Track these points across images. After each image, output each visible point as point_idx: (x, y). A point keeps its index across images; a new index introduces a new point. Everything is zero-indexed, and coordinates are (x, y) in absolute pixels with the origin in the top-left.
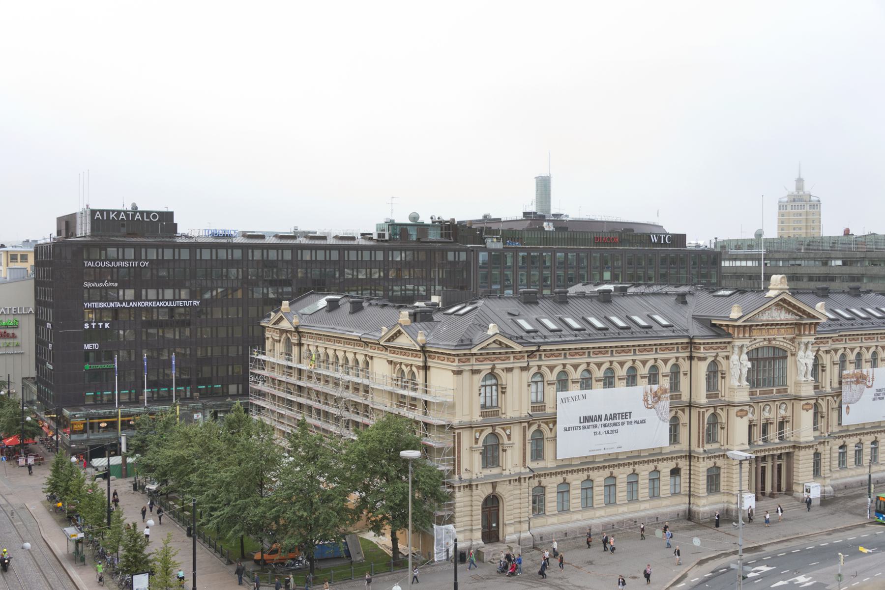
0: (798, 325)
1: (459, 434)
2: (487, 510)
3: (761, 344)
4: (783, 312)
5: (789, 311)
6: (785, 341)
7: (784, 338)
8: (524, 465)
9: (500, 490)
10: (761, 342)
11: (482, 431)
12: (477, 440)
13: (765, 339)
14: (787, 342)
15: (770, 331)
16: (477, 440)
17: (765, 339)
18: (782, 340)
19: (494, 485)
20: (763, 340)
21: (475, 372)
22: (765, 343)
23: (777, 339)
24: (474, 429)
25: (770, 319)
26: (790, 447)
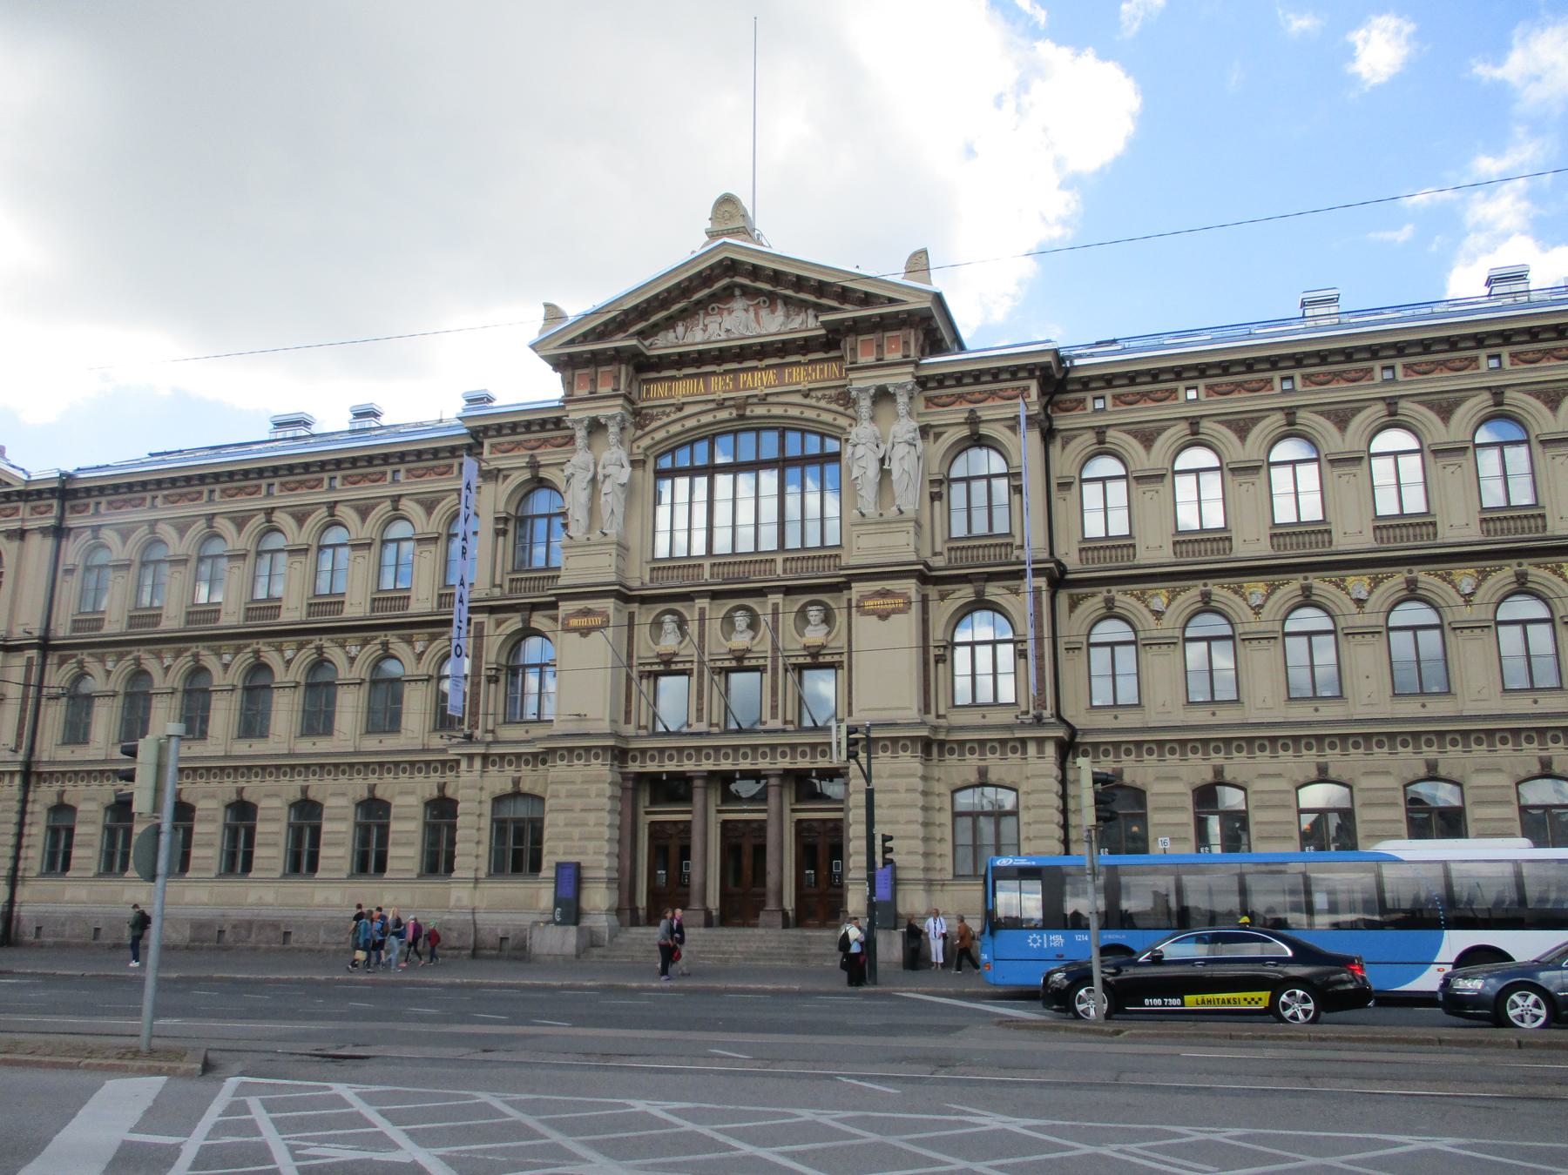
4: (780, 311)
6: (807, 401)
7: (806, 394)
13: (721, 405)
14: (823, 404)
17: (721, 405)
18: (797, 399)
22: (723, 415)
23: (770, 399)
25: (724, 336)
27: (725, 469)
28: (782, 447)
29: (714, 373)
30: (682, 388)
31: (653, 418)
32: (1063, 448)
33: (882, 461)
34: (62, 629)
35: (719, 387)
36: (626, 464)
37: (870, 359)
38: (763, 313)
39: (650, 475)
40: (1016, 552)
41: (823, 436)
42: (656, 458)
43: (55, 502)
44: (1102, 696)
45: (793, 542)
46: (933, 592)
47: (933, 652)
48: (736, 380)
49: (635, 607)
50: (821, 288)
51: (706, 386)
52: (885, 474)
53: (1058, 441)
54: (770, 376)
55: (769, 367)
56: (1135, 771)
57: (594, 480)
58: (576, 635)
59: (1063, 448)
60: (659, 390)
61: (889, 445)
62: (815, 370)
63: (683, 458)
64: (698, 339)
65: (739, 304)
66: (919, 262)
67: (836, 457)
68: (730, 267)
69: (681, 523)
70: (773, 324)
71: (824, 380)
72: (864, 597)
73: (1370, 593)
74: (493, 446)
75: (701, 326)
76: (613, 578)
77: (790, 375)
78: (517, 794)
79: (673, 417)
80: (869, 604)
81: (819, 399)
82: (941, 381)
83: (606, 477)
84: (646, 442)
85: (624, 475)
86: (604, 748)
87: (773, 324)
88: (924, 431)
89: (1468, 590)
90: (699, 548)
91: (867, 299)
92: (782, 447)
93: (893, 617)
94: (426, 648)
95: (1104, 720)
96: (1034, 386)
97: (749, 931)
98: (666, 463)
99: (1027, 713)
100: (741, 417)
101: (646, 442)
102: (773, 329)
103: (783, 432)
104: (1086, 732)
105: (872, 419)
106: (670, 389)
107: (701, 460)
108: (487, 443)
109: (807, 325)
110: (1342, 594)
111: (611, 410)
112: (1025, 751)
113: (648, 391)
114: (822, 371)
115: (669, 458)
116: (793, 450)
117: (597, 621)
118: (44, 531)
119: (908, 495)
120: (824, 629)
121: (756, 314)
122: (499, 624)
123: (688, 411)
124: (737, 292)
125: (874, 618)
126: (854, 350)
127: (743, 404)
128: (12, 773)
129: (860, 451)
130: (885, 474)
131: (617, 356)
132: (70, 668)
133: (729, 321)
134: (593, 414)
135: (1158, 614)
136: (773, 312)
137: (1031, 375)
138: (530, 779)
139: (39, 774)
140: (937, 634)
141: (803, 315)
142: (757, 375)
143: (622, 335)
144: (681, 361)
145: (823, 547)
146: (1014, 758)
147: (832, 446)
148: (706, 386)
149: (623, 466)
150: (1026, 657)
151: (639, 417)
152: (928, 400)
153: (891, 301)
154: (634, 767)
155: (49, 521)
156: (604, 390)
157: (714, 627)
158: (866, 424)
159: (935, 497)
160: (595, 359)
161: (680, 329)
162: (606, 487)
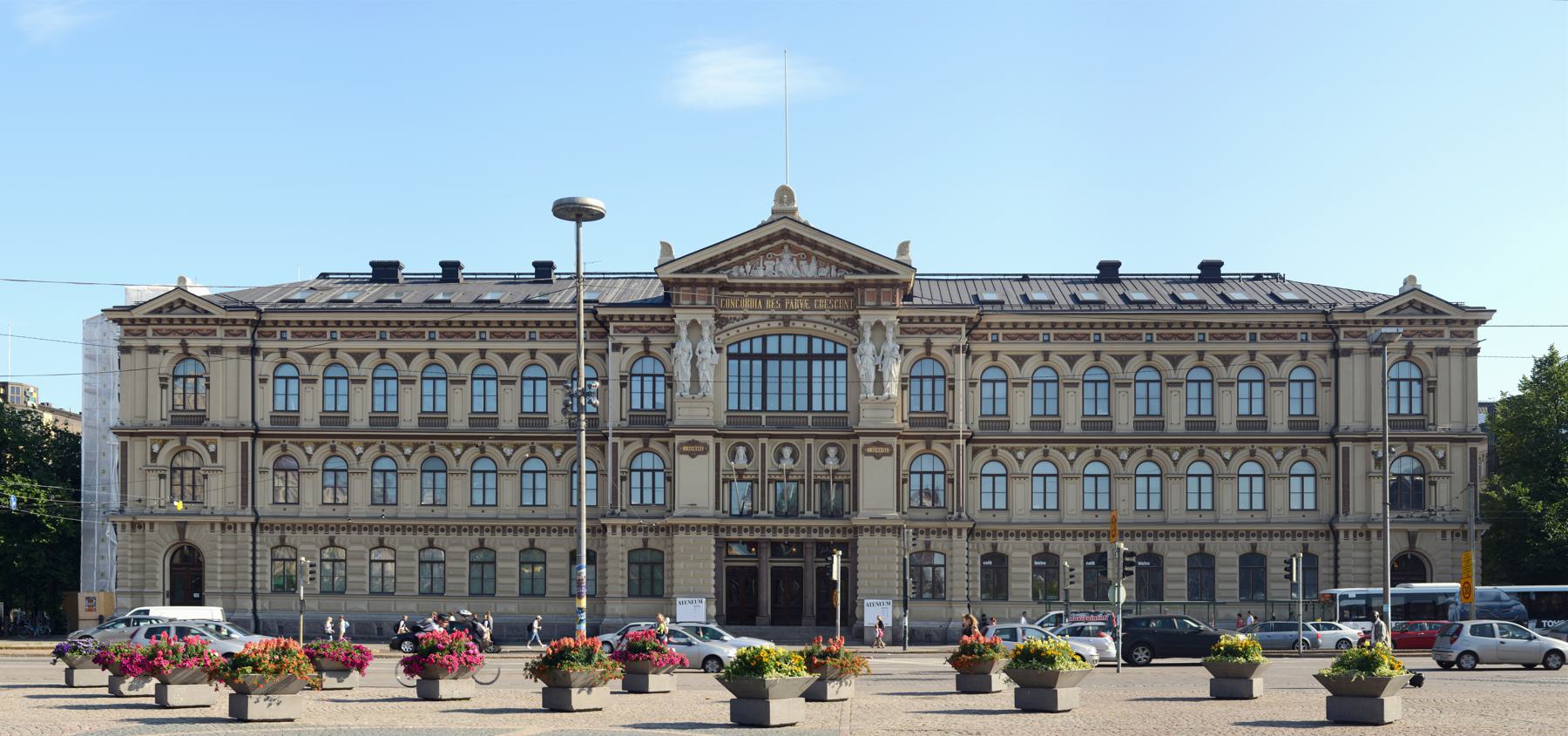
0: (847, 287)
2: (184, 569)
3: (764, 325)
5: (822, 263)
6: (829, 321)
7: (828, 317)
8: (244, 503)
9: (191, 536)
11: (165, 442)
14: (838, 324)
16: (154, 456)
17: (772, 318)
18: (822, 319)
19: (182, 527)
20: (765, 318)
21: (154, 350)
22: (774, 324)
23: (805, 318)
24: (149, 438)
25: (777, 275)
26: (844, 530)
27: (773, 357)
30: (746, 303)
32: (973, 361)
33: (877, 367)
34: (264, 421)
36: (714, 351)
38: (803, 263)
40: (949, 424)
41: (836, 343)
43: (248, 330)
44: (987, 504)
45: (817, 406)
46: (902, 442)
47: (901, 477)
48: (783, 303)
49: (720, 440)
50: (842, 256)
51: (764, 304)
53: (971, 357)
56: (1004, 545)
57: (694, 359)
58: (687, 457)
59: (973, 361)
60: (734, 304)
62: (833, 302)
63: (745, 348)
64: (761, 273)
65: (787, 256)
66: (904, 248)
67: (844, 357)
68: (785, 234)
70: (810, 271)
71: (839, 310)
72: (866, 446)
74: (615, 327)
77: (818, 303)
78: (645, 547)
79: (741, 322)
80: (870, 450)
81: (835, 322)
82: (911, 320)
86: (710, 526)
87: (810, 271)
90: (757, 406)
91: (872, 269)
93: (884, 458)
94: (563, 453)
95: (989, 517)
96: (963, 326)
97: (797, 627)
98: (734, 349)
99: (953, 513)
101: (723, 336)
103: (810, 338)
104: (981, 523)
106: (739, 303)
107: (757, 349)
108: (612, 325)
110: (1114, 456)
111: (706, 317)
112: (951, 534)
113: (724, 303)
114: (838, 303)
116: (817, 349)
118: (242, 350)
119: (893, 389)
120: (836, 460)
121: (798, 263)
122: (626, 444)
123: (750, 320)
124: (786, 247)
126: (863, 297)
128: (243, 525)
130: (879, 375)
131: (709, 284)
132: (275, 451)
133: (782, 268)
135: (1020, 462)
136: (809, 263)
137: (963, 322)
138: (655, 541)
139: (262, 525)
140: (904, 466)
143: (712, 268)
144: (746, 288)
145: (835, 411)
146: (945, 538)
147: (841, 350)
148: (764, 304)
150: (953, 483)
151: (720, 322)
152: (903, 330)
153: (888, 272)
154: (723, 535)
155: (246, 342)
156: (700, 302)
157: (770, 455)
158: (868, 341)
160: (694, 284)
161: (748, 267)
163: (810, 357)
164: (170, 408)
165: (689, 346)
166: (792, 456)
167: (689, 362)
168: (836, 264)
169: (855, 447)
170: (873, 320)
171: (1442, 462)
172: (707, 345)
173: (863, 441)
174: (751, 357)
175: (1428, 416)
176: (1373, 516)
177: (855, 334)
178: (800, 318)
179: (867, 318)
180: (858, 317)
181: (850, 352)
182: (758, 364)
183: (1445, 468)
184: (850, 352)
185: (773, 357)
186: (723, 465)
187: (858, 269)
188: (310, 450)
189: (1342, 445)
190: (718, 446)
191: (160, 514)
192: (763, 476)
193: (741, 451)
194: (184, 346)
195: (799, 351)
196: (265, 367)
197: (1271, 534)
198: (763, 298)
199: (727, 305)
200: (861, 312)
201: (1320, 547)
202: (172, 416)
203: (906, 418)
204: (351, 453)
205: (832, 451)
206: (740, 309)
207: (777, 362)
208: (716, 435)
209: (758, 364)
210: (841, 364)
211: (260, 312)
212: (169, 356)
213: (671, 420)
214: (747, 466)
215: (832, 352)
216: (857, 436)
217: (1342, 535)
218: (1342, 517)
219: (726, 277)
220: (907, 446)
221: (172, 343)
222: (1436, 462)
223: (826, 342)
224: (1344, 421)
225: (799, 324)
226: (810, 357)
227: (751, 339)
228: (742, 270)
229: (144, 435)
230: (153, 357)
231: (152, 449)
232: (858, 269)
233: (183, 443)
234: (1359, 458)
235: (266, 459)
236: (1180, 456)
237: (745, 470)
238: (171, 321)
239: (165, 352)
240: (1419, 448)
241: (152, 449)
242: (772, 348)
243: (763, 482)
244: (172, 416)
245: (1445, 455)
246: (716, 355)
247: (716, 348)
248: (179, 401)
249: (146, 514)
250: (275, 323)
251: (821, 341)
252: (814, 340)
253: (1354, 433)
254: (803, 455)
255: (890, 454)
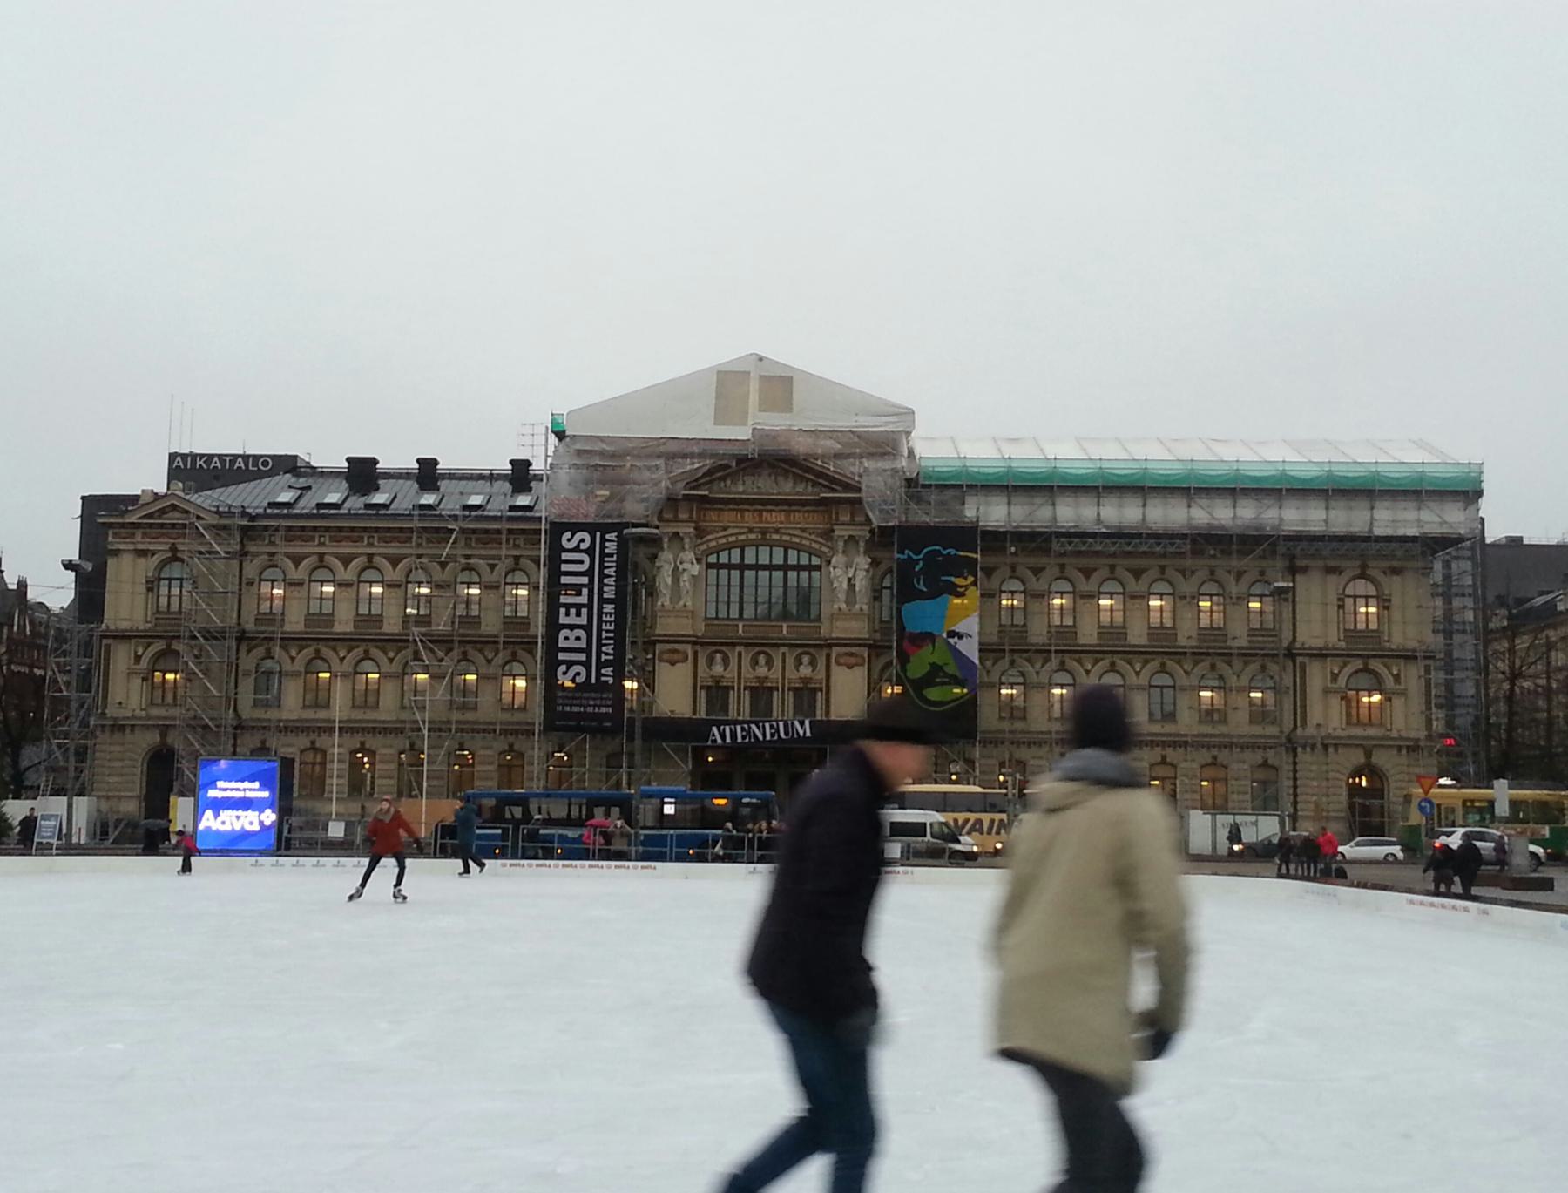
0: (824, 502)
1: (108, 647)
5: (799, 479)
7: (803, 530)
10: (743, 533)
11: (149, 645)
12: (138, 659)
13: (751, 530)
14: (813, 537)
15: (764, 514)
16: (138, 659)
17: (751, 530)
20: (746, 530)
22: (752, 536)
23: (783, 531)
24: (133, 641)
25: (755, 490)
27: (750, 567)
28: (786, 559)
29: (748, 510)
30: (728, 517)
31: (709, 534)
33: (850, 579)
34: (250, 626)
35: (750, 519)
37: (847, 518)
38: (781, 479)
39: (704, 567)
41: (810, 554)
42: (707, 556)
48: (761, 516)
49: (698, 647)
51: (742, 517)
52: (851, 586)
54: (782, 517)
55: (781, 511)
57: (676, 568)
58: (667, 664)
61: (853, 570)
63: (724, 558)
64: (741, 489)
67: (819, 568)
69: (722, 598)
73: (1093, 667)
75: (741, 482)
76: (691, 632)
79: (721, 534)
83: (684, 570)
84: (704, 547)
85: (695, 569)
88: (875, 563)
89: (1138, 669)
90: (734, 614)
92: (786, 559)
93: (856, 668)
98: (712, 559)
100: (765, 539)
102: (788, 491)
105: (844, 552)
107: (736, 559)
109: (806, 492)
111: (688, 529)
113: (704, 515)
115: (715, 555)
116: (792, 561)
117: (679, 657)
118: (230, 555)
120: (810, 669)
121: (776, 479)
123: (730, 531)
125: (845, 668)
126: (837, 514)
127: (764, 532)
129: (839, 572)
130: (851, 586)
134: (675, 530)
139: (243, 728)
141: (803, 485)
142: (774, 514)
147: (816, 561)
148: (742, 517)
149: (692, 563)
151: (700, 533)
156: (683, 516)
157: (746, 661)
158: (840, 555)
159: (875, 599)
161: (729, 482)
162: (685, 577)
163: (785, 568)
164: (155, 610)
165: (671, 557)
166: (767, 663)
167: (670, 573)
168: (812, 480)
169: (828, 656)
170: (846, 534)
171: (1397, 678)
172: (689, 555)
173: (835, 651)
174: (729, 566)
175: (1383, 633)
176: (1330, 731)
177: (829, 547)
178: (777, 531)
179: (841, 532)
180: (833, 531)
181: (824, 564)
182: (735, 574)
183: (1400, 683)
184: (824, 564)
185: (750, 567)
186: (700, 674)
187: (833, 486)
188: (293, 653)
189: (1299, 659)
190: (696, 653)
191: (140, 718)
192: (739, 684)
193: (718, 656)
194: (174, 549)
195: (775, 562)
196: (251, 570)
197: (1230, 746)
198: (742, 511)
199: (708, 518)
200: (835, 527)
201: (1281, 759)
202: (157, 619)
203: (877, 628)
204: (335, 656)
205: (806, 659)
206: (719, 521)
207: (754, 572)
208: (694, 643)
209: (735, 574)
210: (816, 574)
211: (253, 518)
212: (155, 560)
213: (651, 627)
214: (723, 673)
215: (807, 563)
216: (830, 646)
217: (1299, 749)
218: (1299, 730)
219: (707, 493)
220: (878, 656)
221: (162, 546)
222: (1391, 678)
223: (801, 553)
224: (1300, 638)
225: (776, 537)
226: (785, 568)
227: (730, 549)
228: (722, 484)
229: (129, 637)
230: (142, 561)
231: (136, 652)
232: (833, 486)
233: (169, 645)
234: (1317, 676)
235: (248, 662)
236: (1141, 669)
237: (723, 677)
238: (162, 526)
239: (153, 555)
240: (1375, 665)
241: (136, 652)
242: (750, 558)
243: (739, 689)
244: (157, 619)
245: (1399, 670)
246: (697, 567)
247: (697, 559)
248: (163, 601)
249: (128, 718)
250: (266, 528)
251: (796, 552)
252: (790, 551)
253: (1311, 648)
254: (778, 663)
255: (862, 665)
